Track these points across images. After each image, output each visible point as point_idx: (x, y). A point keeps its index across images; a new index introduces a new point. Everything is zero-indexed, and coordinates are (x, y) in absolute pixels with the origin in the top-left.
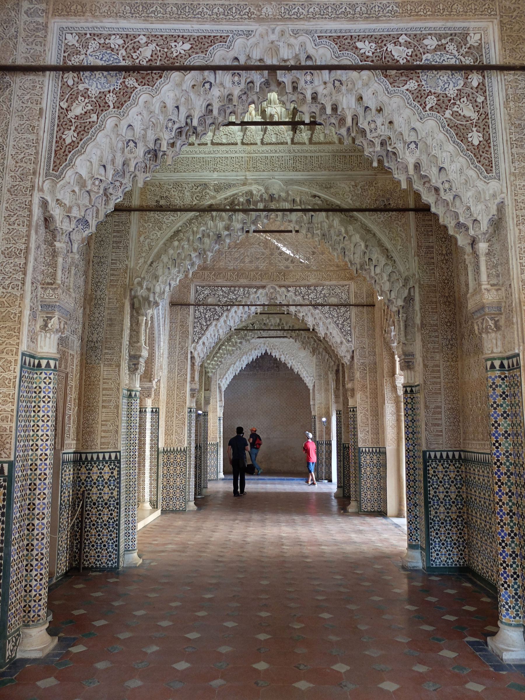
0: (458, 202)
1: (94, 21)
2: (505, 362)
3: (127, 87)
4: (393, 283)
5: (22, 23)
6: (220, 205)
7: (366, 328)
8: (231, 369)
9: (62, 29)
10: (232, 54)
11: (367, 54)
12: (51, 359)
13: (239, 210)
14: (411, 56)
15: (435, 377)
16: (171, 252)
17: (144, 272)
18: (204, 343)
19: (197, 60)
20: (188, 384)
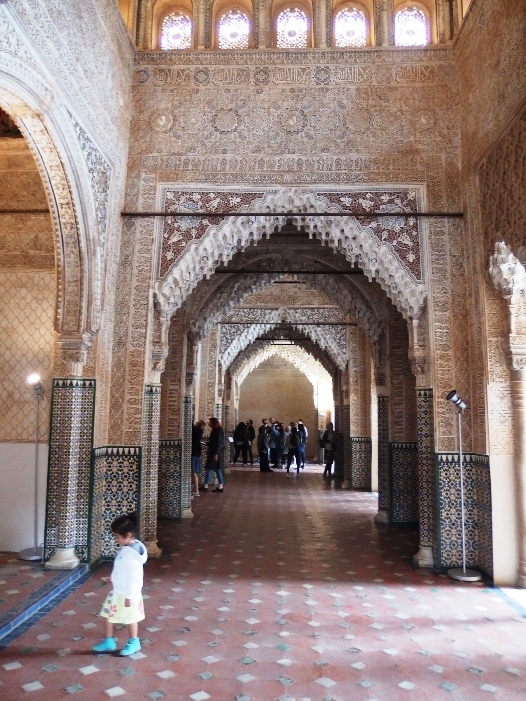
0: (401, 295)
2: (427, 392)
9: (164, 189)
18: (229, 353)
19: (244, 209)
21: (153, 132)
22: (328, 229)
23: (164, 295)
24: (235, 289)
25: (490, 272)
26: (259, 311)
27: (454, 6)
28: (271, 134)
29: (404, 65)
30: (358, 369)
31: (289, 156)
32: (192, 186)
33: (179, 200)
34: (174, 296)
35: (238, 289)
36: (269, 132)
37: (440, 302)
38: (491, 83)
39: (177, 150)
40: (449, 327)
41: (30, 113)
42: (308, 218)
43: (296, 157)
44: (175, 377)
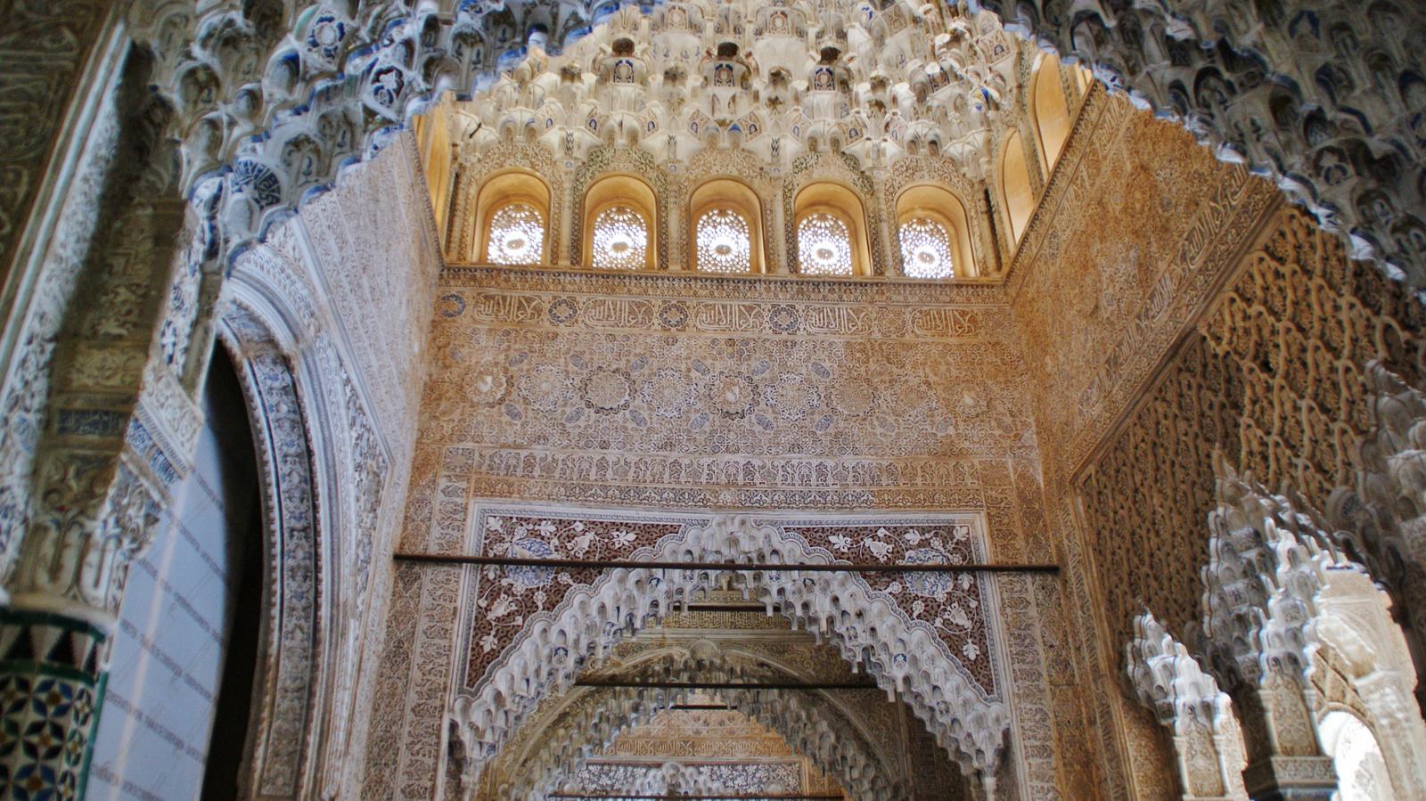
0: (957, 727)
6: (626, 675)
13: (654, 685)
16: (554, 744)
19: (643, 555)
21: (467, 405)
22: (806, 597)
23: (473, 727)
25: (1130, 675)
26: (622, 769)
27: (996, 221)
28: (693, 417)
31: (728, 457)
32: (538, 508)
33: (511, 533)
34: (493, 728)
36: (688, 412)
37: (1035, 737)
38: (1086, 340)
39: (511, 440)
40: (1058, 788)
41: (272, 353)
42: (766, 574)
43: (741, 458)
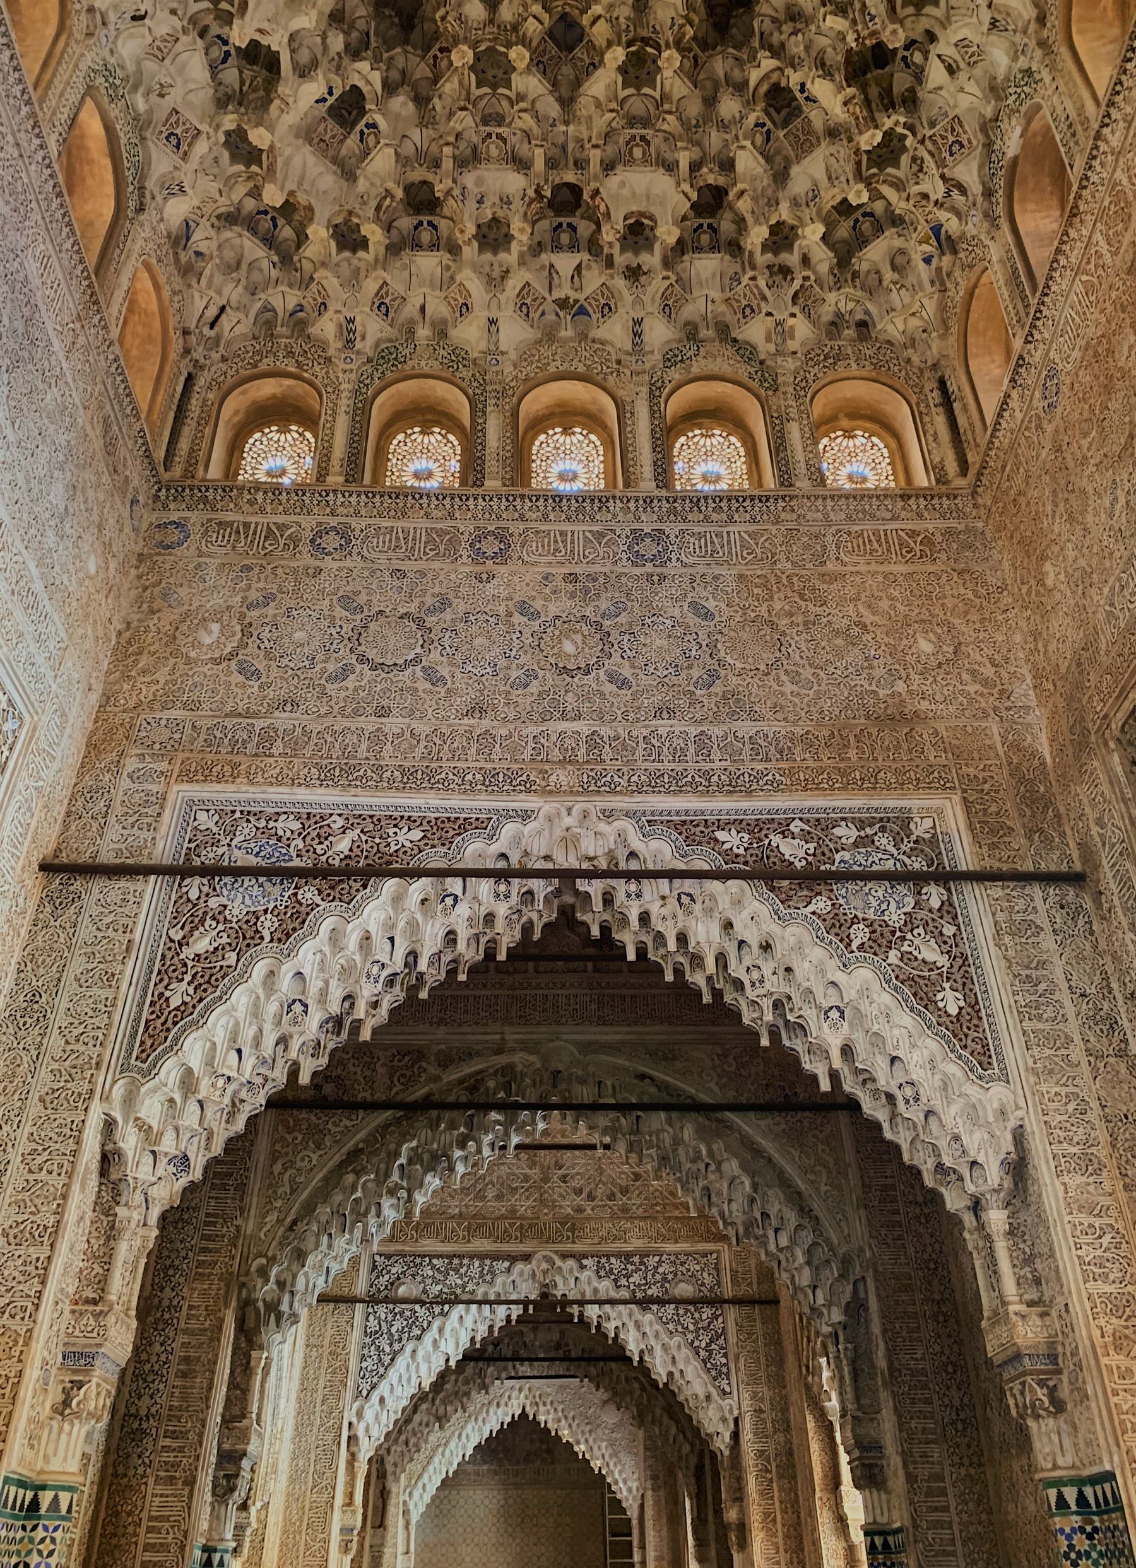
1: (252, 789)
2: (1088, 1491)
3: (301, 904)
4: (817, 1268)
5: (121, 793)
7: (763, 1360)
8: (436, 1460)
10: (496, 848)
11: (735, 850)
12: (64, 1488)
14: (814, 855)
15: (936, 1509)
17: (274, 1244)
18: (382, 1400)
20: (337, 1514)
23: (144, 1129)
24: (402, 1160)
29: (856, 528)
30: (771, 1449)
34: (177, 1129)
35: (410, 1161)
40: (1120, 1226)
43: (583, 727)
44: (176, 1465)
